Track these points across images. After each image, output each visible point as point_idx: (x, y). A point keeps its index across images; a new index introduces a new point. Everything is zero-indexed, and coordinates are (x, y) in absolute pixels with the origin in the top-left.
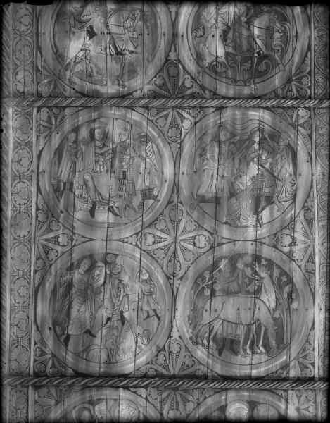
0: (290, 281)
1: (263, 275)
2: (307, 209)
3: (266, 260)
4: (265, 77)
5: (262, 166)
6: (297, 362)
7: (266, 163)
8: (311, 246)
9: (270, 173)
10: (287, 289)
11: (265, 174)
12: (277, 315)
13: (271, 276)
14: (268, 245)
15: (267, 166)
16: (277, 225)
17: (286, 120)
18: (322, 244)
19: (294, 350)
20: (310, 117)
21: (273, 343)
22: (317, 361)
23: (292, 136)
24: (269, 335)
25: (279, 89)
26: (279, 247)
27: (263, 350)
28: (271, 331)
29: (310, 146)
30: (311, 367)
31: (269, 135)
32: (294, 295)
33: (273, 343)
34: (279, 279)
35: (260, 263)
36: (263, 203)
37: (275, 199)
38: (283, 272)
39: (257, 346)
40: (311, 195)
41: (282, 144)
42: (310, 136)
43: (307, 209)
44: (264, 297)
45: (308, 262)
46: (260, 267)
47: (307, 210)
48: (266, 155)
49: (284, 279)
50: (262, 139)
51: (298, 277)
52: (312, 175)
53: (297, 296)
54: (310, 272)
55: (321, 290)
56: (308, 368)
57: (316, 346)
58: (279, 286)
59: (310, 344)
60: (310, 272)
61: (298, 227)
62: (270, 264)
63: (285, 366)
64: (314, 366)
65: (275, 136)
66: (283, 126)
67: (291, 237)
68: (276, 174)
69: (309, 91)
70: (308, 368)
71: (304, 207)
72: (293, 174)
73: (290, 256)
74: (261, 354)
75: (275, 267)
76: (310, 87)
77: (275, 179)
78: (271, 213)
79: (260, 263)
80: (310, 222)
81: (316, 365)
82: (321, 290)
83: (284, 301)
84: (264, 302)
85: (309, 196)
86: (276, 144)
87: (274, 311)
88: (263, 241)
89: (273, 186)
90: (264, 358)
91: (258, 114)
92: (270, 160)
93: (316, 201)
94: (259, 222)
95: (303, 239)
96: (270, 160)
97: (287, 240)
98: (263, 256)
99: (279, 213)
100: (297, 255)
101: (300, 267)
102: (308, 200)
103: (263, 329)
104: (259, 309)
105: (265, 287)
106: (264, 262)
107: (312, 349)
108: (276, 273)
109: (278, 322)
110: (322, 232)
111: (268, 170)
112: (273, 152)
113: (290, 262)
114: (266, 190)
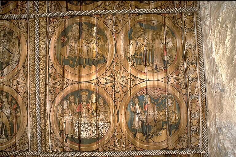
0: (16, 102)
1: (4, 100)
2: (24, 67)
3: (6, 92)
4: (6, 5)
5: (5, 47)
6: (20, 142)
7: (6, 46)
8: (26, 85)
9: (8, 51)
10: (14, 107)
11: (6, 51)
12: (10, 119)
13: (8, 100)
14: (6, 85)
15: (7, 47)
16: (11, 75)
17: (16, 25)
18: (31, 84)
19: (19, 135)
20: (27, 23)
21: (9, 133)
22: (29, 142)
23: (19, 32)
24: (7, 129)
25: (12, 10)
26: (11, 86)
27: (5, 137)
28: (8, 127)
29: (26, 37)
30: (27, 144)
31: (8, 33)
32: (18, 110)
33: (9, 133)
34: (11, 102)
35: (2, 94)
36: (5, 65)
37: (10, 63)
38: (13, 98)
39: (2, 134)
40: (27, 60)
41: (14, 36)
42: (27, 32)
43: (24, 67)
44: (4, 110)
45: (24, 93)
46: (2, 96)
47: (24, 68)
48: (6, 42)
49: (14, 102)
50: (5, 35)
51: (20, 99)
52: (27, 50)
53: (20, 110)
54: (25, 98)
55: (30, 106)
56: (25, 145)
57: (29, 134)
58: (11, 105)
59: (26, 133)
60: (25, 98)
61: (20, 76)
62: (7, 95)
63: (15, 144)
64: (28, 144)
65: (11, 33)
66: (15, 28)
67: (17, 81)
68: (11, 51)
69: (26, 10)
70: (25, 145)
71: (23, 66)
72: (18, 50)
73: (16, 90)
74: (4, 138)
75: (9, 96)
76: (27, 9)
77: (10, 53)
78: (8, 69)
79: (2, 94)
80: (25, 73)
81: (29, 143)
82: (30, 106)
83: (13, 112)
84: (5, 113)
85: (25, 61)
86: (11, 37)
87: (9, 117)
88: (4, 83)
89: (10, 56)
90: (5, 140)
91: (3, 22)
92: (8, 44)
93: (29, 63)
94: (2, 74)
95: (22, 81)
96: (8, 44)
97: (15, 83)
98: (4, 90)
99: (11, 70)
100: (20, 89)
101: (21, 95)
102: (25, 63)
103: (4, 126)
104: (2, 117)
105: (5, 106)
106: (4, 94)
107: (27, 135)
108: (10, 98)
109: (11, 123)
110: (31, 78)
111: (7, 49)
112: (10, 41)
113: (16, 93)
114: (6, 59)
